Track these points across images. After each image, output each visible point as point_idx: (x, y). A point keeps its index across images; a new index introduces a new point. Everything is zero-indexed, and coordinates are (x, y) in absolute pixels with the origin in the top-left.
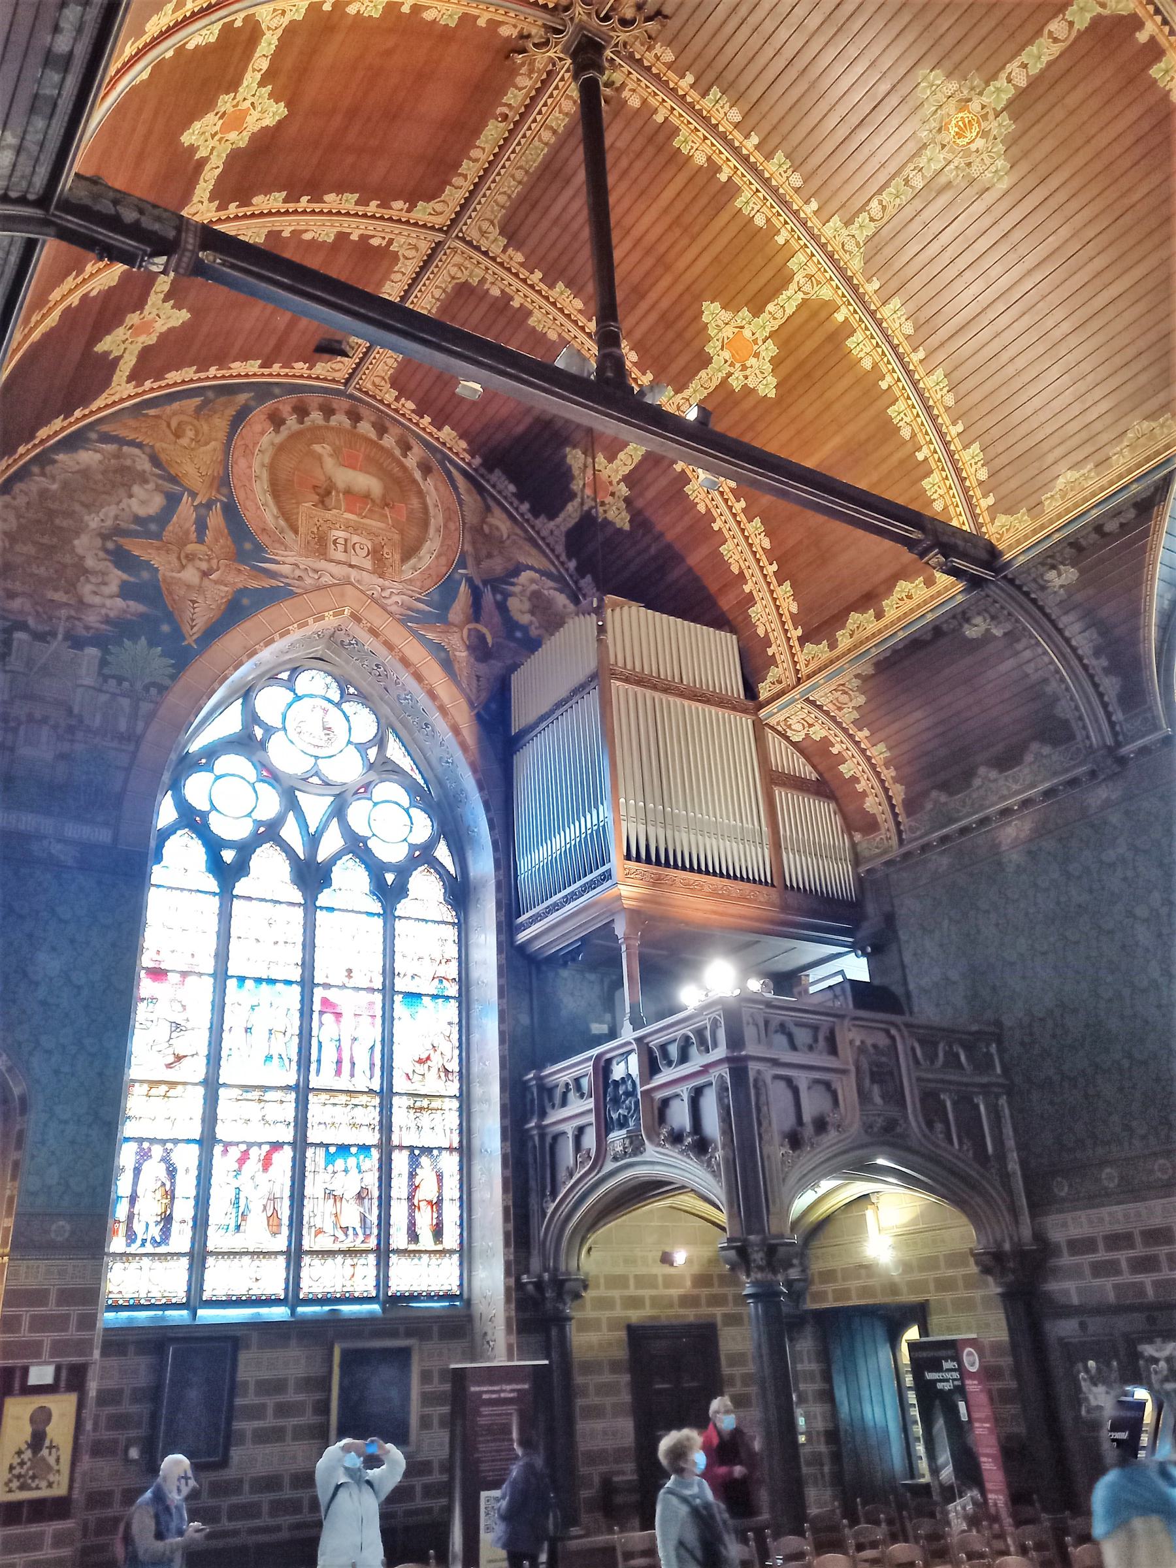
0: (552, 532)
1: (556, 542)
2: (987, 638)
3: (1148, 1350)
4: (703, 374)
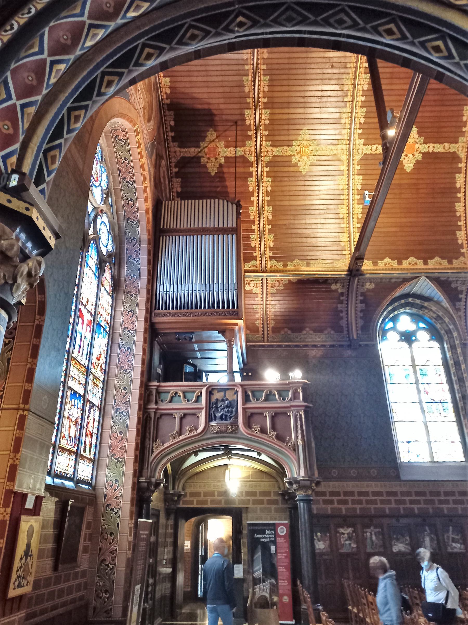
0: (175, 152)
1: (174, 157)
2: (336, 291)
3: (341, 530)
4: (285, 148)
